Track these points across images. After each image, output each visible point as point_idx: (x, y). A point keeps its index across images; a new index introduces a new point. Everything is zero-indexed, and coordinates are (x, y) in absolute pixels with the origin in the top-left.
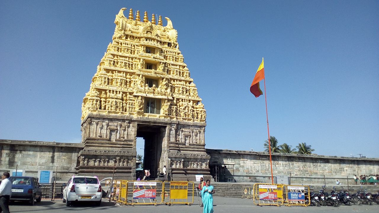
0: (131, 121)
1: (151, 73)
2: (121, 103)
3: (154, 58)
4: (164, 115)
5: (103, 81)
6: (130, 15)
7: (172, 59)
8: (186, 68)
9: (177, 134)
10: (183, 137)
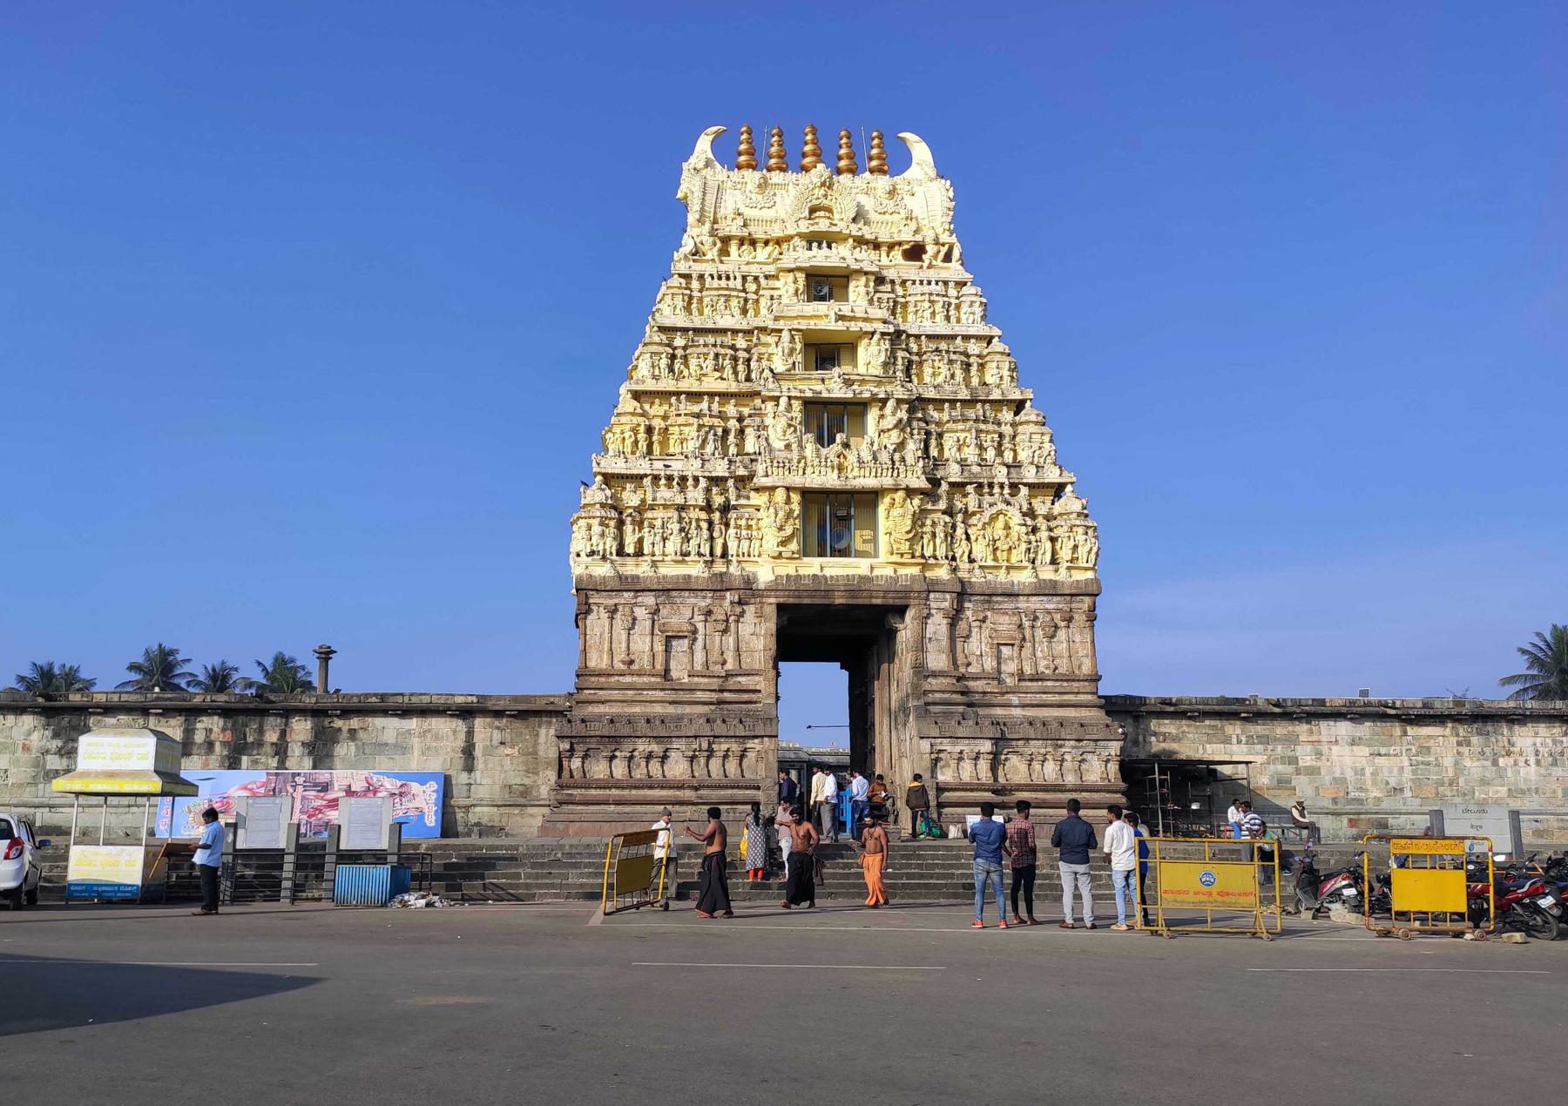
0: (748, 591)
2: (704, 525)
3: (841, 318)
5: (629, 442)
6: (740, 154)
7: (927, 314)
8: (997, 345)
9: (954, 637)
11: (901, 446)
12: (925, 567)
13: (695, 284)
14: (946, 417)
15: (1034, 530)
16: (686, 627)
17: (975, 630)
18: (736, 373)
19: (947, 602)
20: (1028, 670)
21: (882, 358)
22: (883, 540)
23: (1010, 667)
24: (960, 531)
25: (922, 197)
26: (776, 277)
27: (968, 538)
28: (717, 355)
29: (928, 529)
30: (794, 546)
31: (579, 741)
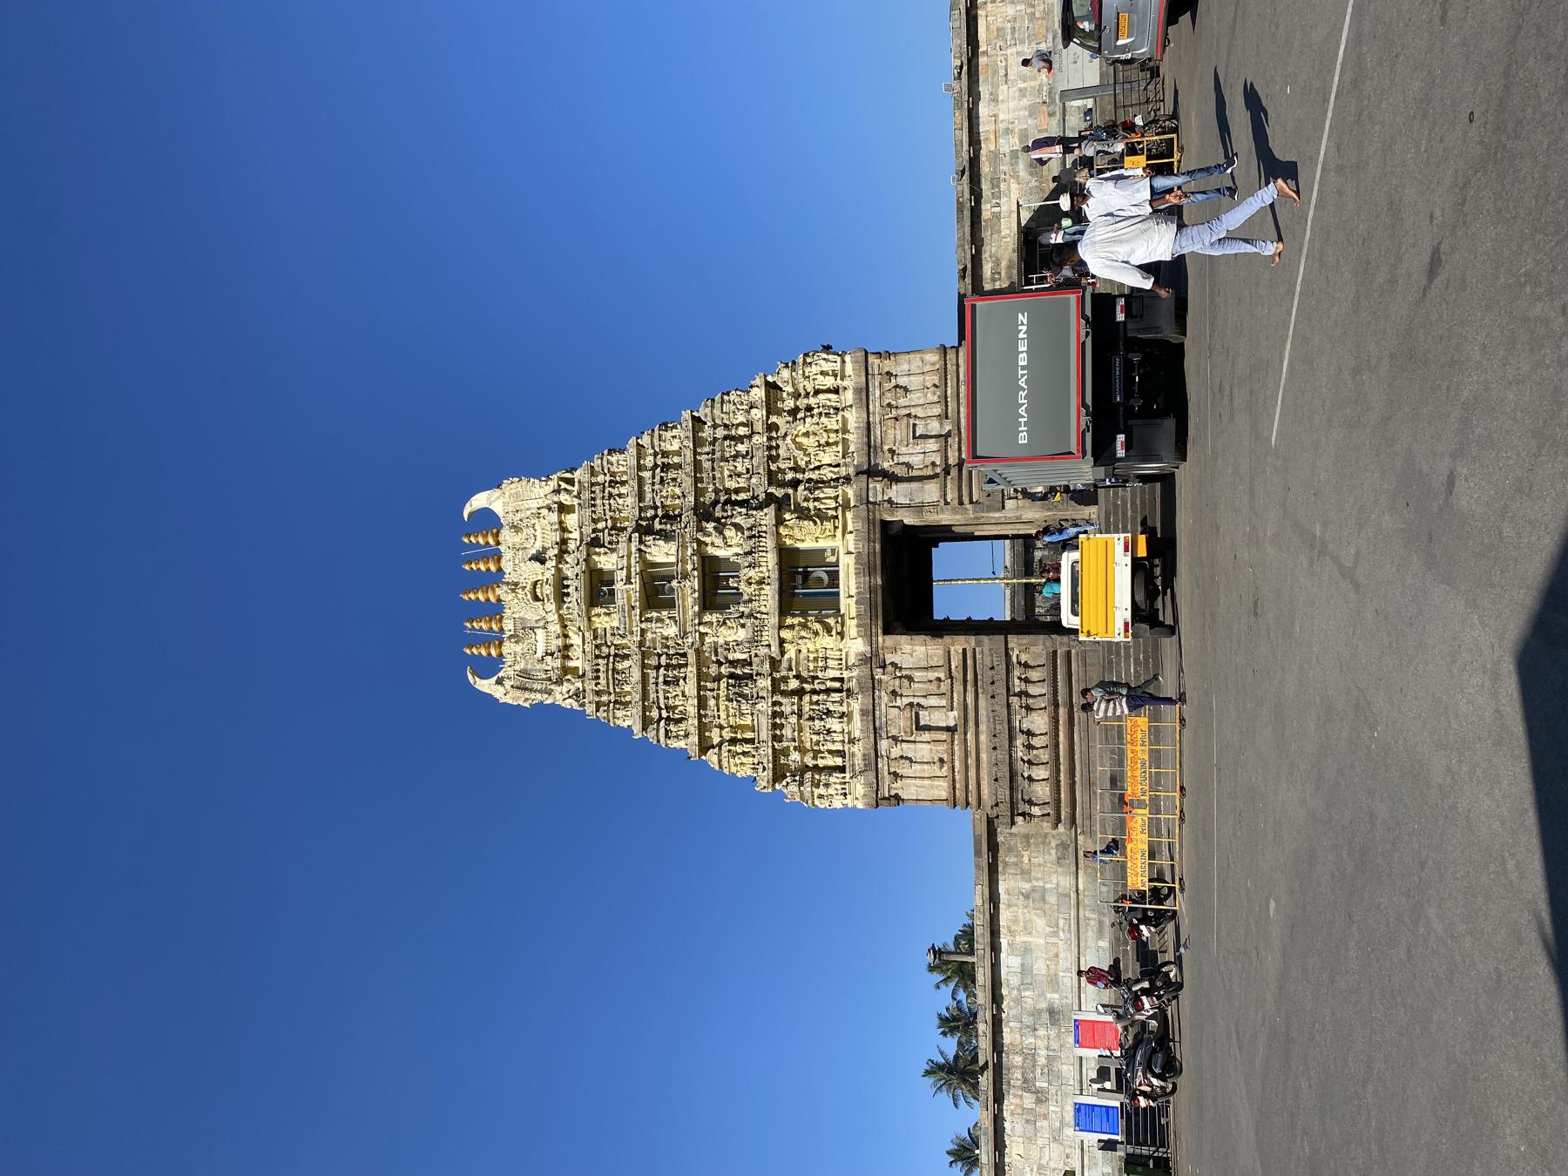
0: (873, 660)
1: (688, 592)
2: (815, 698)
3: (628, 581)
4: (839, 531)
5: (744, 760)
7: (621, 501)
8: (645, 440)
10: (919, 449)
11: (738, 527)
12: (846, 506)
13: (604, 698)
14: (711, 488)
15: (809, 409)
16: (907, 713)
17: (902, 459)
18: (680, 666)
19: (877, 486)
20: (937, 410)
21: (661, 543)
22: (822, 544)
23: (935, 427)
24: (814, 475)
25: (522, 510)
26: (595, 631)
27: (818, 468)
28: (666, 683)
29: (811, 505)
30: (831, 621)
31: (1017, 807)
